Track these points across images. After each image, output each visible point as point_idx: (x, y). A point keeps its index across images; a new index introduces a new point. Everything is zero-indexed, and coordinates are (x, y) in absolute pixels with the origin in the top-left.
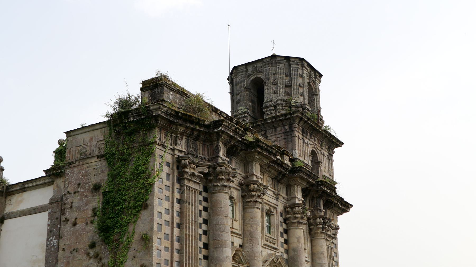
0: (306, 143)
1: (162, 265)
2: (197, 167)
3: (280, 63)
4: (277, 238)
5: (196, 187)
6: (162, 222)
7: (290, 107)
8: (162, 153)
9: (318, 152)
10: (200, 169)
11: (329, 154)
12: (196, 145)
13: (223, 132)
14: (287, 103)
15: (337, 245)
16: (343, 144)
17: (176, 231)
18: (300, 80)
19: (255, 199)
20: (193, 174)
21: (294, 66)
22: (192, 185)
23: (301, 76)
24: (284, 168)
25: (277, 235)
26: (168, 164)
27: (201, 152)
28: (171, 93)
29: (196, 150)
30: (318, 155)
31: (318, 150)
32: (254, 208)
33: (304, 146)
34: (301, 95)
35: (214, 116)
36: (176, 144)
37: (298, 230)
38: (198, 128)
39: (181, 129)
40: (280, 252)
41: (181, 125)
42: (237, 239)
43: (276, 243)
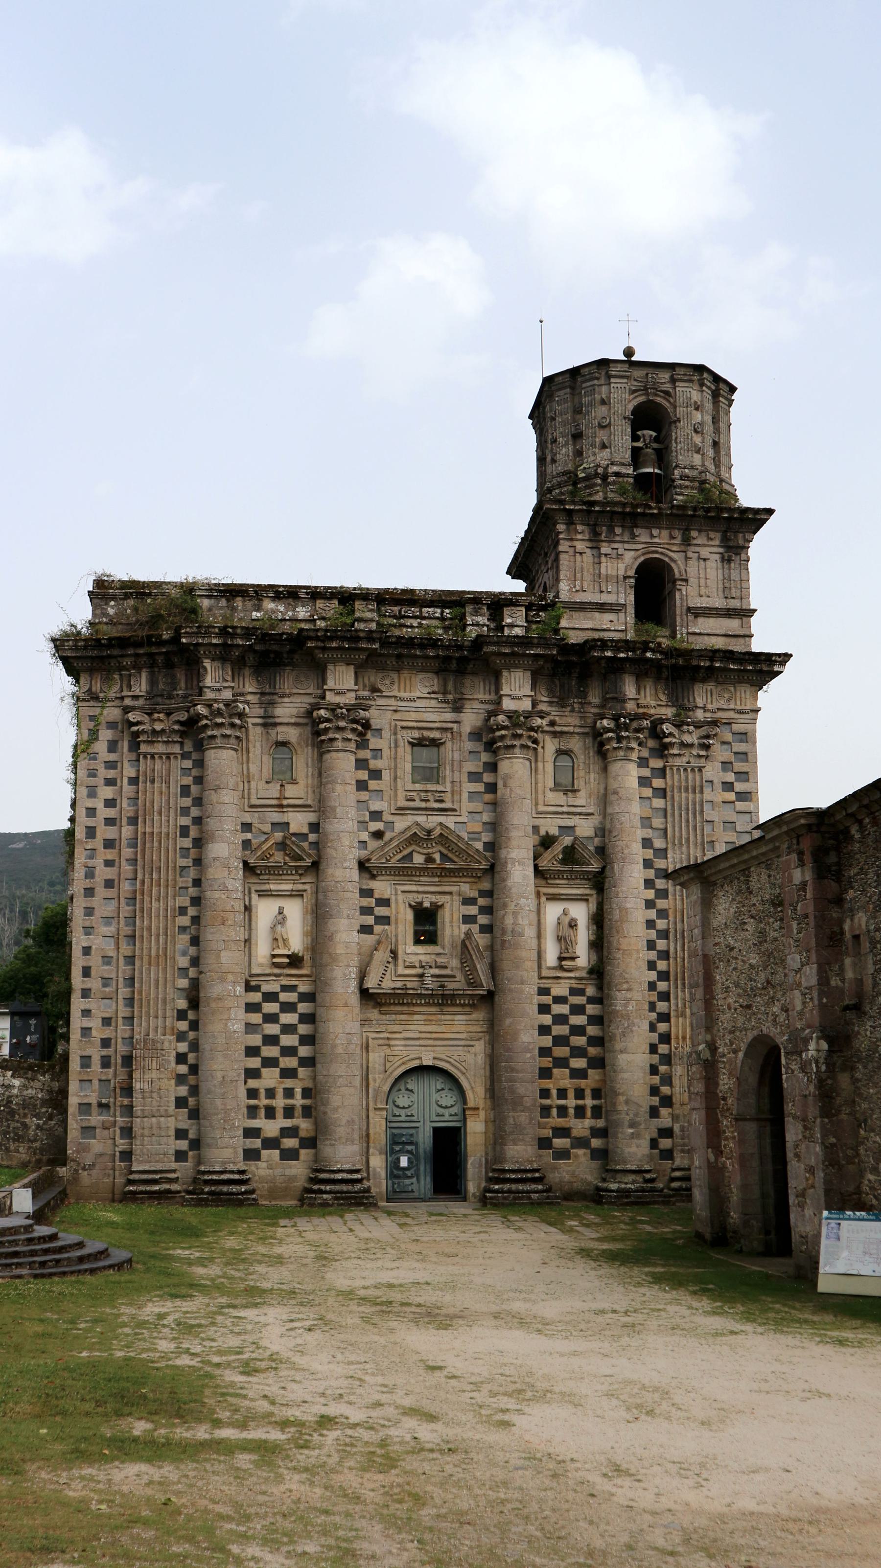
0: (606, 555)
1: (97, 890)
2: (168, 714)
3: (560, 389)
4: (453, 787)
5: (176, 749)
6: (98, 822)
7: (575, 481)
8: (97, 711)
9: (671, 559)
10: (175, 717)
11: (729, 548)
12: (174, 677)
13: (198, 644)
14: (569, 478)
15: (750, 755)
16: (770, 512)
17: (127, 831)
18: (604, 409)
19: (331, 735)
20: (154, 731)
21: (588, 384)
22: (160, 748)
23: (603, 402)
24: (448, 648)
25: (452, 782)
26: (112, 725)
27: (183, 685)
28: (112, 603)
29: (174, 685)
30: (673, 565)
31: (671, 554)
32: (329, 751)
33: (600, 563)
34: (604, 446)
35: (240, 604)
36: (130, 687)
37: (506, 762)
38: (154, 650)
39: (128, 662)
40: (464, 813)
41: (122, 656)
42: (298, 814)
43: (447, 797)
